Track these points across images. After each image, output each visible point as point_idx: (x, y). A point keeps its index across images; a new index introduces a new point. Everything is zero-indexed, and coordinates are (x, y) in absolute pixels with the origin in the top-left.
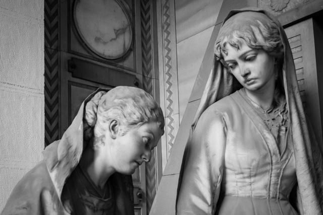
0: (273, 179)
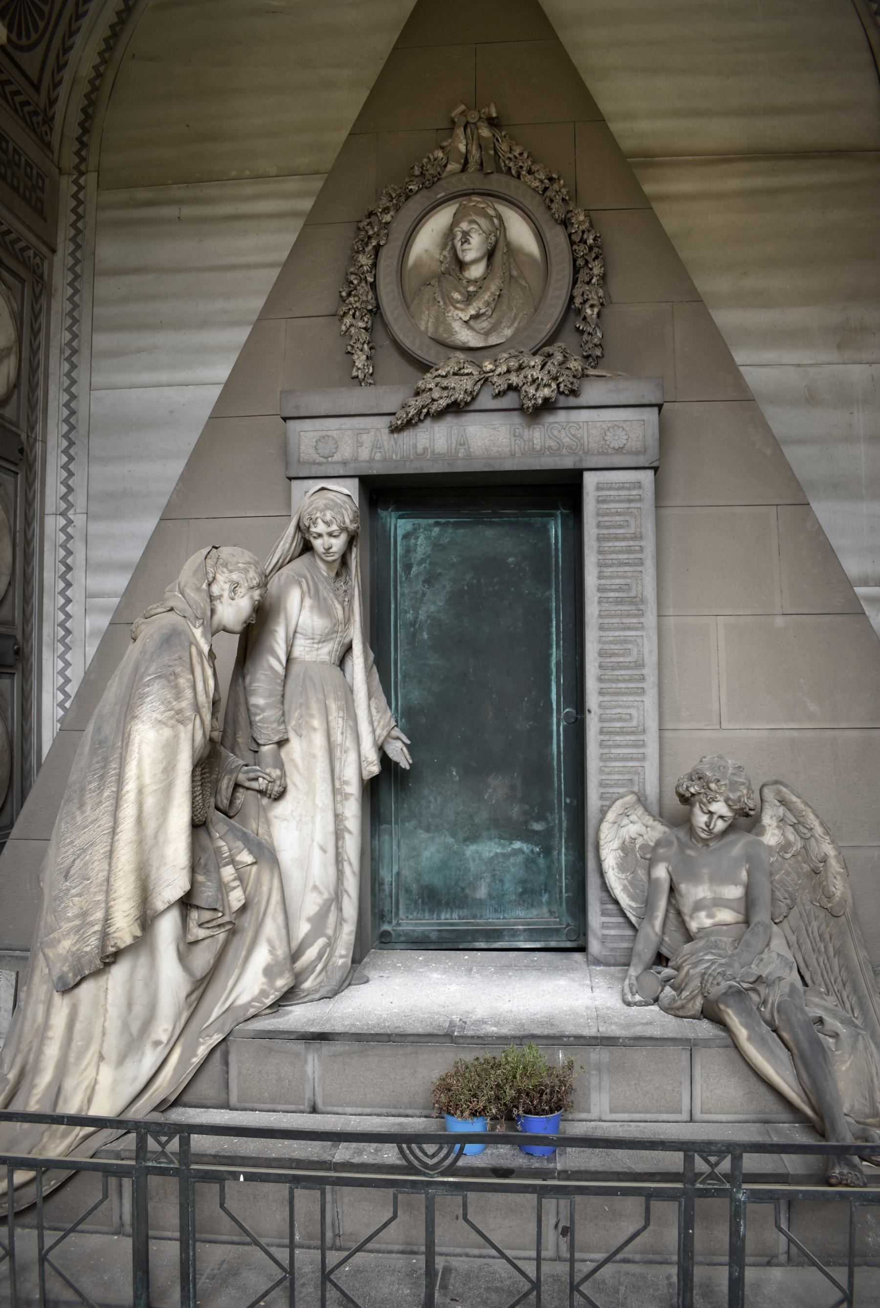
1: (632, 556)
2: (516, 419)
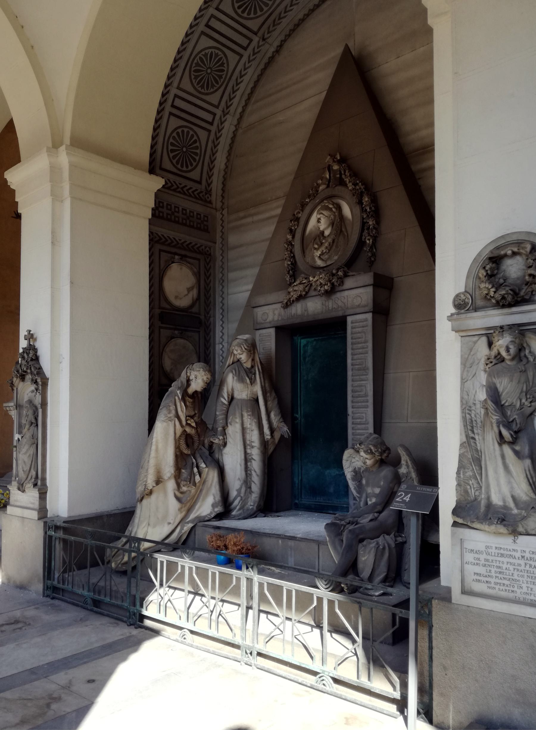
0: (249, 392)
1: (364, 350)
2: (324, 298)
